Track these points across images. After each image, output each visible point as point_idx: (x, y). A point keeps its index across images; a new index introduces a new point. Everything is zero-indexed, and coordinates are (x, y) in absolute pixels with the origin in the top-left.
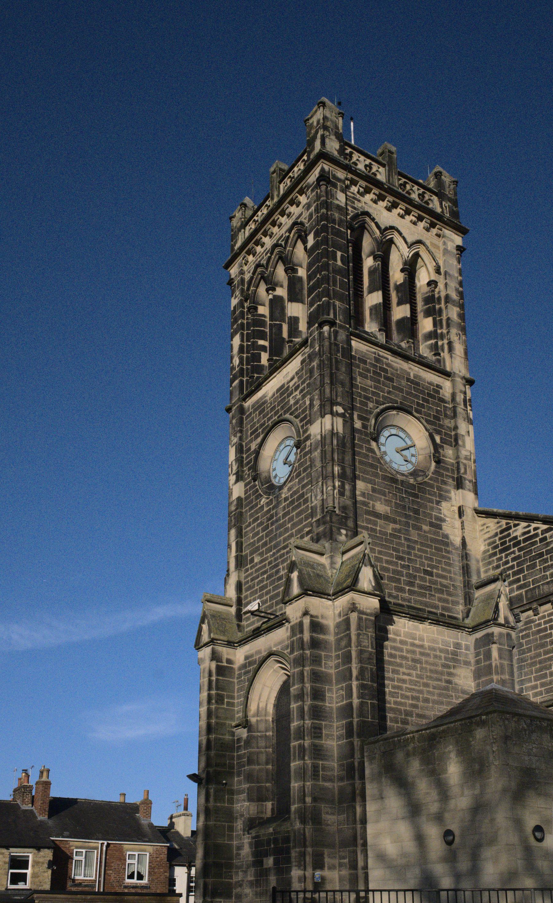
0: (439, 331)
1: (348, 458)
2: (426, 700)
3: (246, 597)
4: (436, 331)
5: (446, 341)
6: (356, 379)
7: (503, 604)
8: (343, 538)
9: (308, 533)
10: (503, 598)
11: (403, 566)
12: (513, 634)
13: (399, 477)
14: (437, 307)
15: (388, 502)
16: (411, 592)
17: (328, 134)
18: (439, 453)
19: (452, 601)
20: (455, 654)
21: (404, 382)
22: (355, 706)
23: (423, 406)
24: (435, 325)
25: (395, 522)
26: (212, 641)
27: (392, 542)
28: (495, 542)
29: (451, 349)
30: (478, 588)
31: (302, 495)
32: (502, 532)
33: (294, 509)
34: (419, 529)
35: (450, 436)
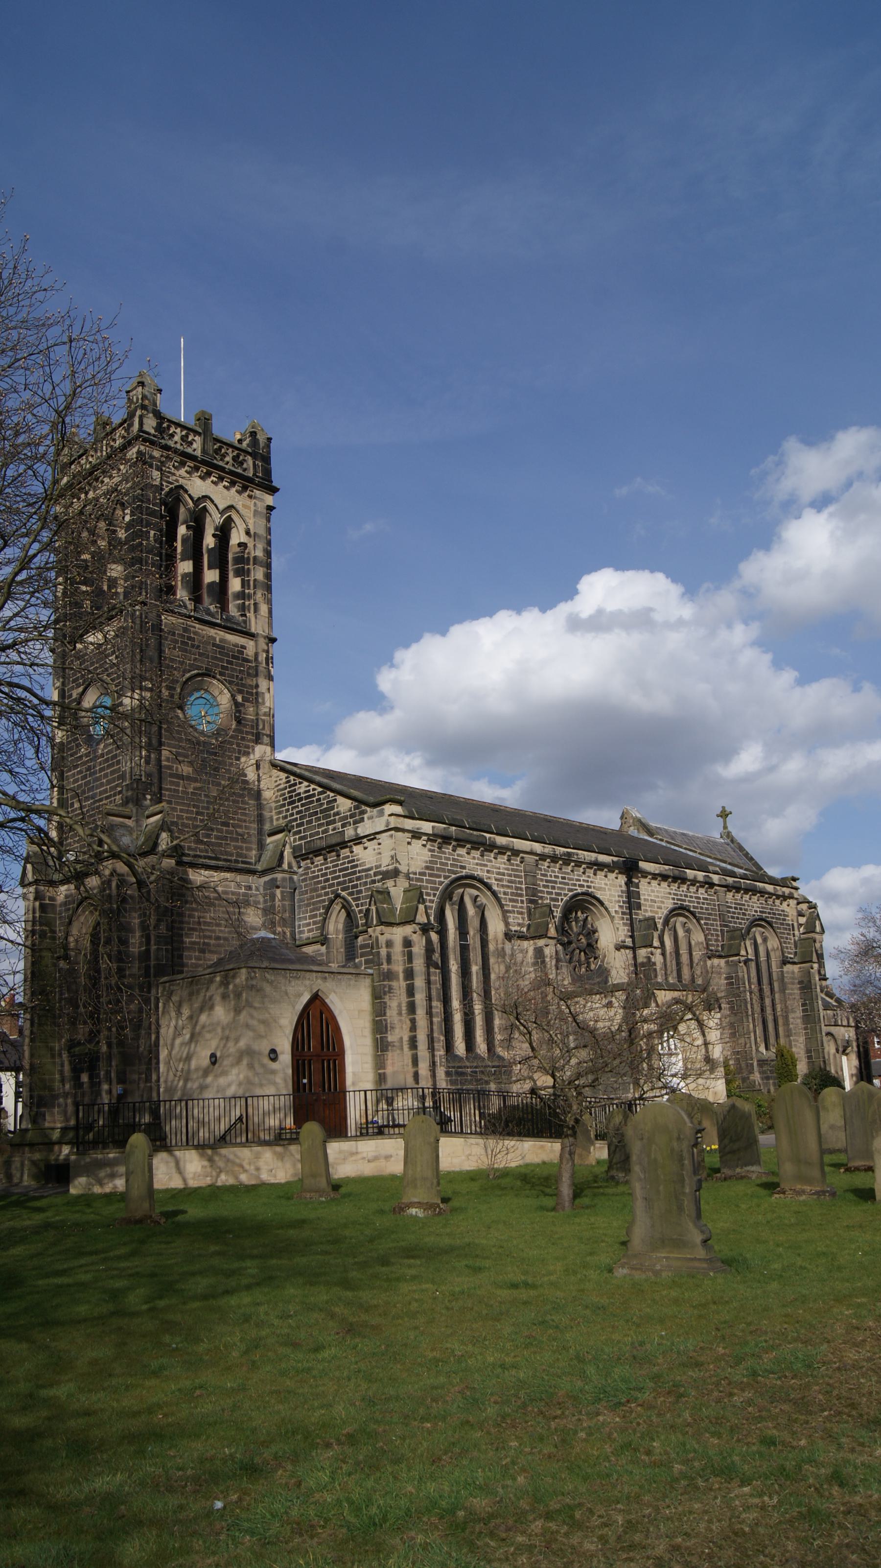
0: (247, 591)
2: (218, 938)
3: (66, 839)
4: (243, 592)
5: (252, 602)
7: (287, 851)
8: (148, 802)
9: (120, 792)
10: (288, 846)
12: (295, 877)
14: (246, 567)
15: (191, 763)
17: (146, 412)
18: (240, 712)
19: (246, 848)
20: (245, 895)
21: (210, 647)
22: (152, 951)
23: (226, 668)
24: (243, 586)
25: (195, 780)
26: (36, 882)
28: (284, 794)
29: (256, 610)
30: (270, 835)
31: (115, 756)
32: (290, 786)
33: (109, 767)
34: (219, 784)
35: (252, 694)
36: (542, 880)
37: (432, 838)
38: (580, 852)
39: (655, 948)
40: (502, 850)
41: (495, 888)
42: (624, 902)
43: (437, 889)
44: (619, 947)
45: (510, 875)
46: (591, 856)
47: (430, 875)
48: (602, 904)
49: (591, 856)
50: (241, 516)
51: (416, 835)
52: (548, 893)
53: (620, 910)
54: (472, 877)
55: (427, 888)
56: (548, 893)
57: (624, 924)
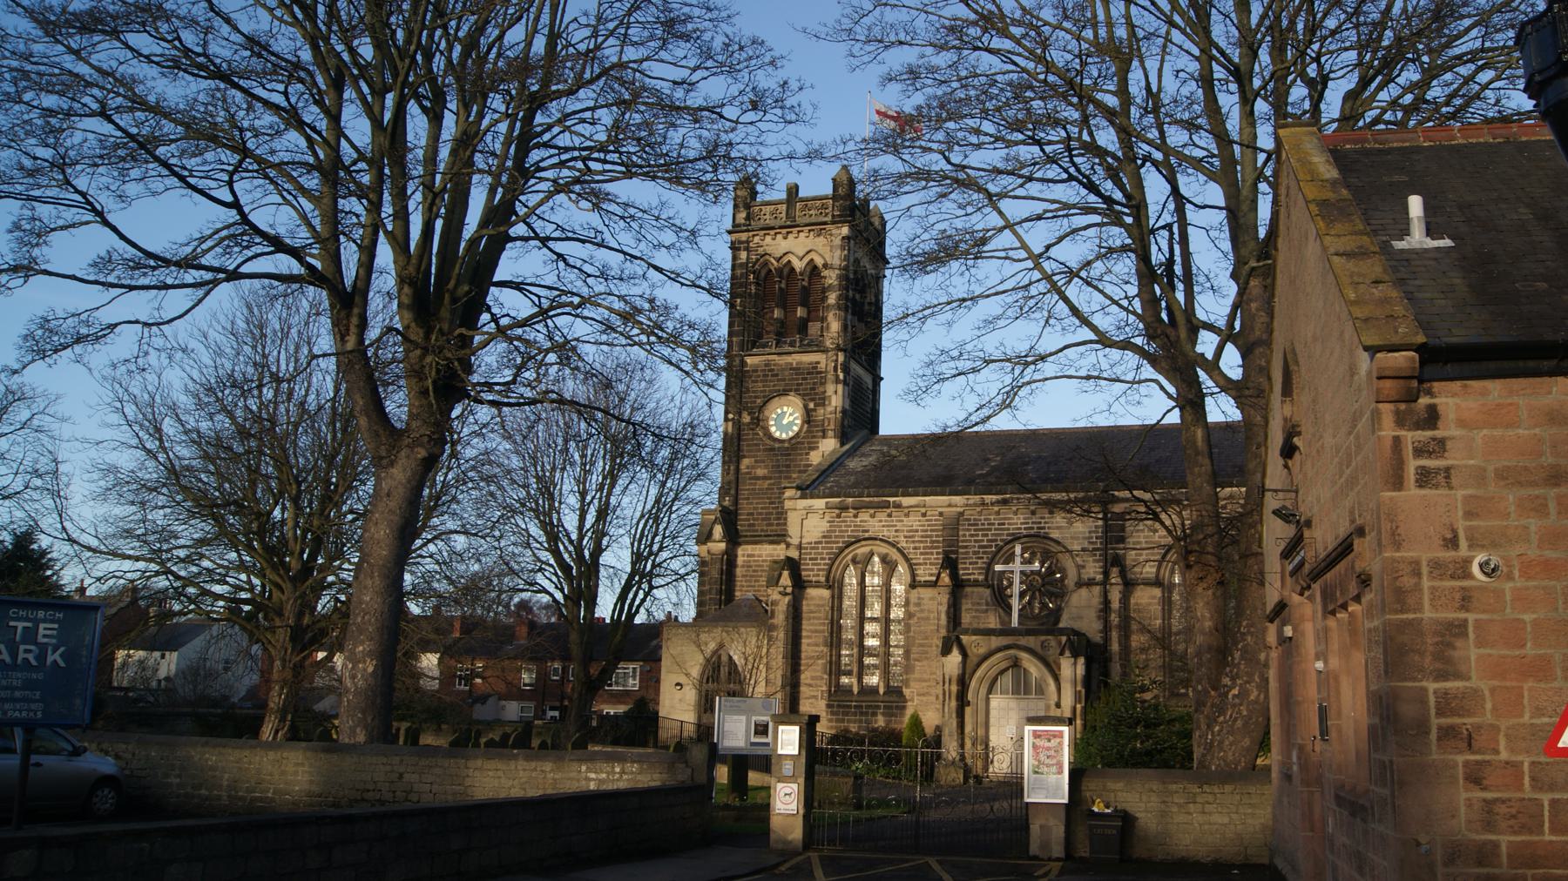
13: (777, 445)
15: (766, 467)
16: (778, 525)
25: (770, 478)
34: (790, 477)
44: (1080, 584)
51: (809, 511)
52: (976, 541)
54: (875, 539)
56: (976, 541)
57: (1095, 561)
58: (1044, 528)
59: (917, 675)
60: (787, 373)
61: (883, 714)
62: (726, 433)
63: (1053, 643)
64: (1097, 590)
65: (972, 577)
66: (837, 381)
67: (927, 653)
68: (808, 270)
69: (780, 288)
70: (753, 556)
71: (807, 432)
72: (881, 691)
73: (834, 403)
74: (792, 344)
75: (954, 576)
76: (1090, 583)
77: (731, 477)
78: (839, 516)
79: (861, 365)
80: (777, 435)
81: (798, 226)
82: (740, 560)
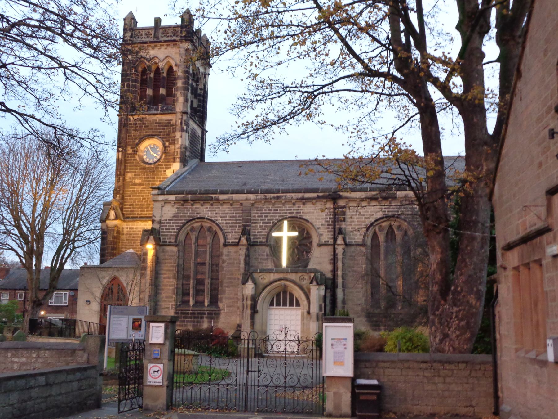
1: (123, 167)
6: (131, 133)
11: (145, 202)
15: (141, 178)
16: (147, 211)
23: (162, 132)
25: (143, 185)
27: (141, 193)
36: (257, 213)
37: (177, 201)
38: (288, 194)
39: (338, 245)
40: (224, 202)
41: (219, 221)
42: (330, 218)
43: (178, 226)
44: (320, 245)
45: (231, 214)
46: (300, 195)
47: (175, 220)
48: (308, 221)
49: (300, 195)
50: (173, 59)
51: (166, 202)
52: (261, 220)
53: (326, 224)
54: (204, 218)
55: (173, 226)
57: (328, 231)
58: (300, 213)
59: (226, 295)
60: (153, 125)
61: (207, 318)
62: (118, 160)
63: (306, 277)
64: (330, 248)
65: (259, 240)
66: (182, 130)
67: (232, 283)
68: (167, 67)
69: (150, 77)
70: (133, 228)
71: (165, 159)
72: (206, 304)
73: (180, 143)
74: (157, 109)
75: (248, 240)
76: (326, 244)
77: (120, 184)
78: (183, 205)
79: (195, 122)
80: (147, 160)
81: (161, 42)
82: (125, 231)
